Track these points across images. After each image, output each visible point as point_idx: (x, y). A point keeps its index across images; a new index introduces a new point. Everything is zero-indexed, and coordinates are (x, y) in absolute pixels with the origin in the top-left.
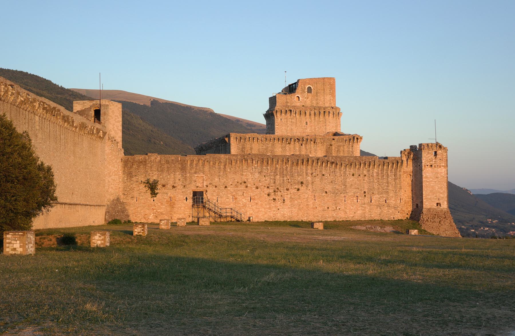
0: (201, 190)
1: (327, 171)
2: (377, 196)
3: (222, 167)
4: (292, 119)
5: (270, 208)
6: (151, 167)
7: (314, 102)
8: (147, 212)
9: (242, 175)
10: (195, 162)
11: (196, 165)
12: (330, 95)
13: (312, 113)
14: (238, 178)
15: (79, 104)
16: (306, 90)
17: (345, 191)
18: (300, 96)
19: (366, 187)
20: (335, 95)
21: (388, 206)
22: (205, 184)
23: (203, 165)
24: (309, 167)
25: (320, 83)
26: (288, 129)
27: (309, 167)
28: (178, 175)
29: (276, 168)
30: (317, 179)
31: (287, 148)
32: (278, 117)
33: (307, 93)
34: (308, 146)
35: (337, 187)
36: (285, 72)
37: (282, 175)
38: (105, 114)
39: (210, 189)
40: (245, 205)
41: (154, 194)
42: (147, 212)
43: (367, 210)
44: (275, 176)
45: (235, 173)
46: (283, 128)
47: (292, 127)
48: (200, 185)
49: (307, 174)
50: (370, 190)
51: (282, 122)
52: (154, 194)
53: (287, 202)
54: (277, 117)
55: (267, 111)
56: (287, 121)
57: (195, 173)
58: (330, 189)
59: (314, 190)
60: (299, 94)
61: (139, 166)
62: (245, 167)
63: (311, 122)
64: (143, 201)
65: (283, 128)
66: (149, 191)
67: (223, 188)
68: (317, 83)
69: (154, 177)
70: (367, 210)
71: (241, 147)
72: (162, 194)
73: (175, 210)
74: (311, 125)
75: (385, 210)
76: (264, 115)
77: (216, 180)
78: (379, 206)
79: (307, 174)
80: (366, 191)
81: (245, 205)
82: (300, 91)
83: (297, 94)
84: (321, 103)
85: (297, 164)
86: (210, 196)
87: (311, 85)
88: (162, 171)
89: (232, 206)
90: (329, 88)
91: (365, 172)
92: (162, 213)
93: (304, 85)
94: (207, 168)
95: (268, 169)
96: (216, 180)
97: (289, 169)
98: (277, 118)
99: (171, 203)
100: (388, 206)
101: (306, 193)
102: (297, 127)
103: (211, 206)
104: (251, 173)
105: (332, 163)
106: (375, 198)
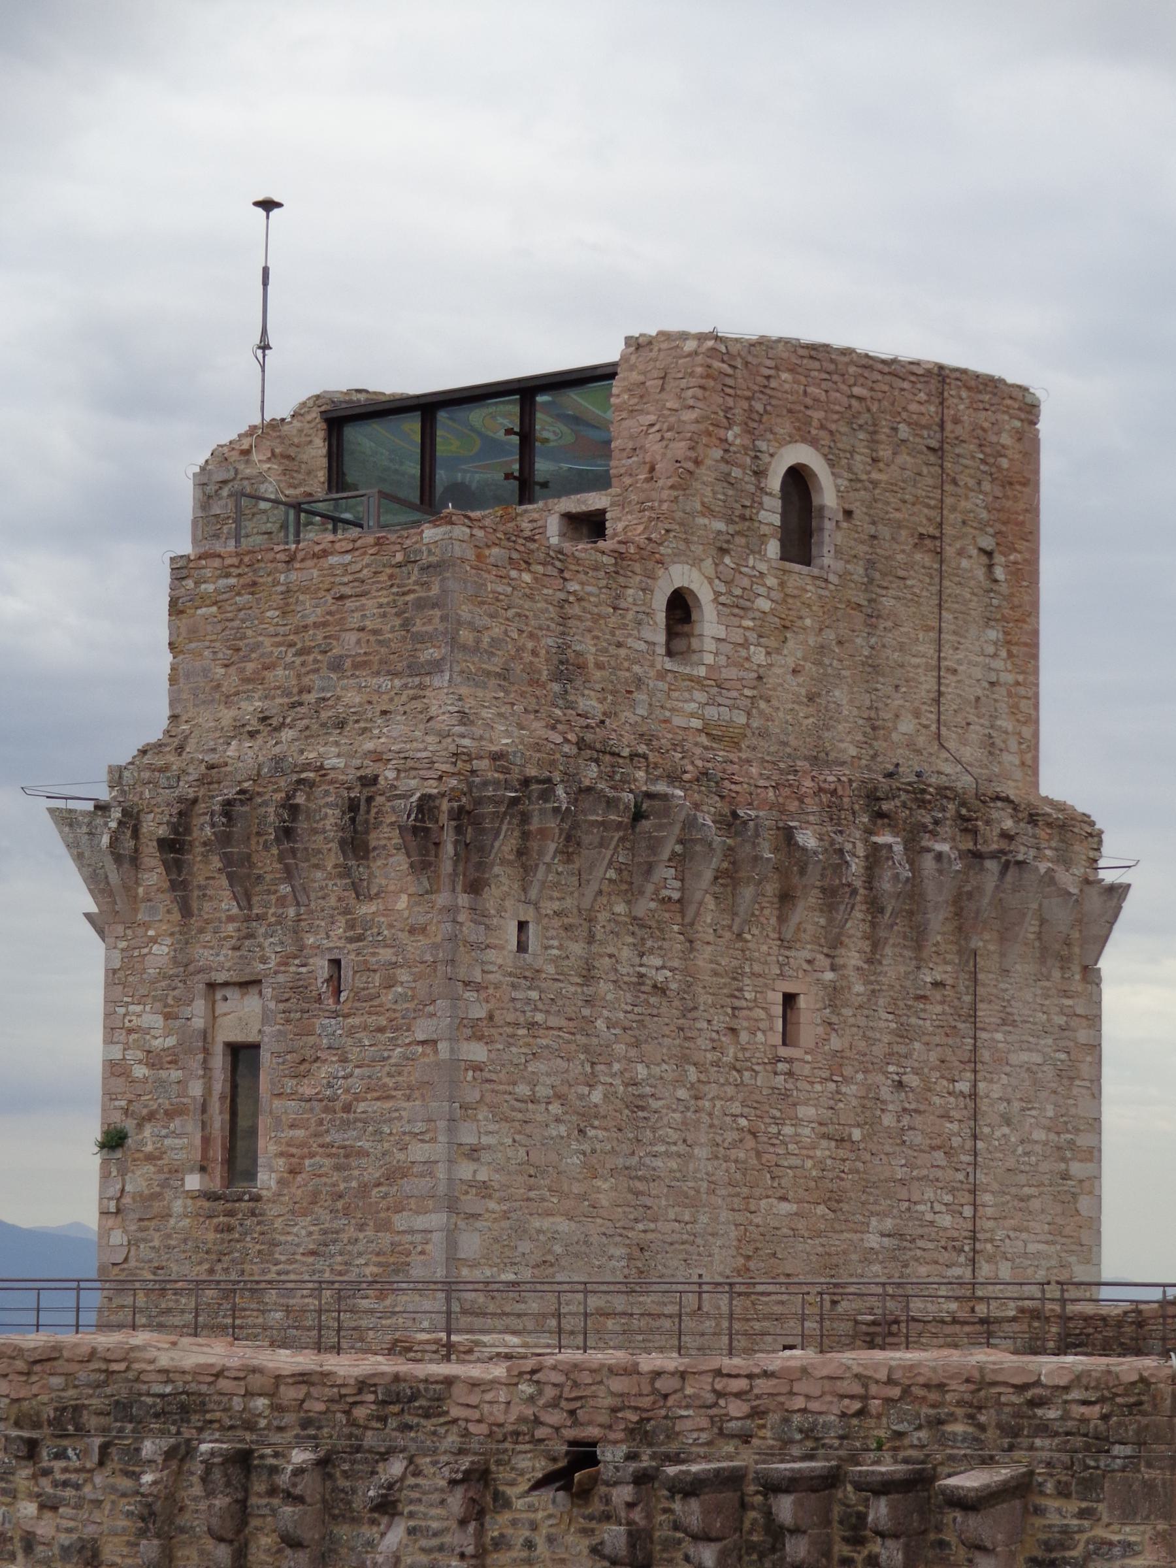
7: (839, 694)
12: (988, 621)
18: (704, 593)
20: (1036, 633)
25: (904, 431)
26: (597, 1096)
32: (491, 898)
33: (773, 548)
36: (268, 205)
47: (641, 1071)
51: (532, 977)
54: (475, 887)
55: (124, 755)
56: (588, 975)
60: (696, 562)
63: (834, 995)
68: (873, 442)
74: (836, 1043)
76: (65, 819)
82: (708, 511)
83: (677, 556)
84: (907, 726)
87: (814, 443)
90: (982, 527)
93: (754, 425)
98: (479, 915)
102: (692, 1074)
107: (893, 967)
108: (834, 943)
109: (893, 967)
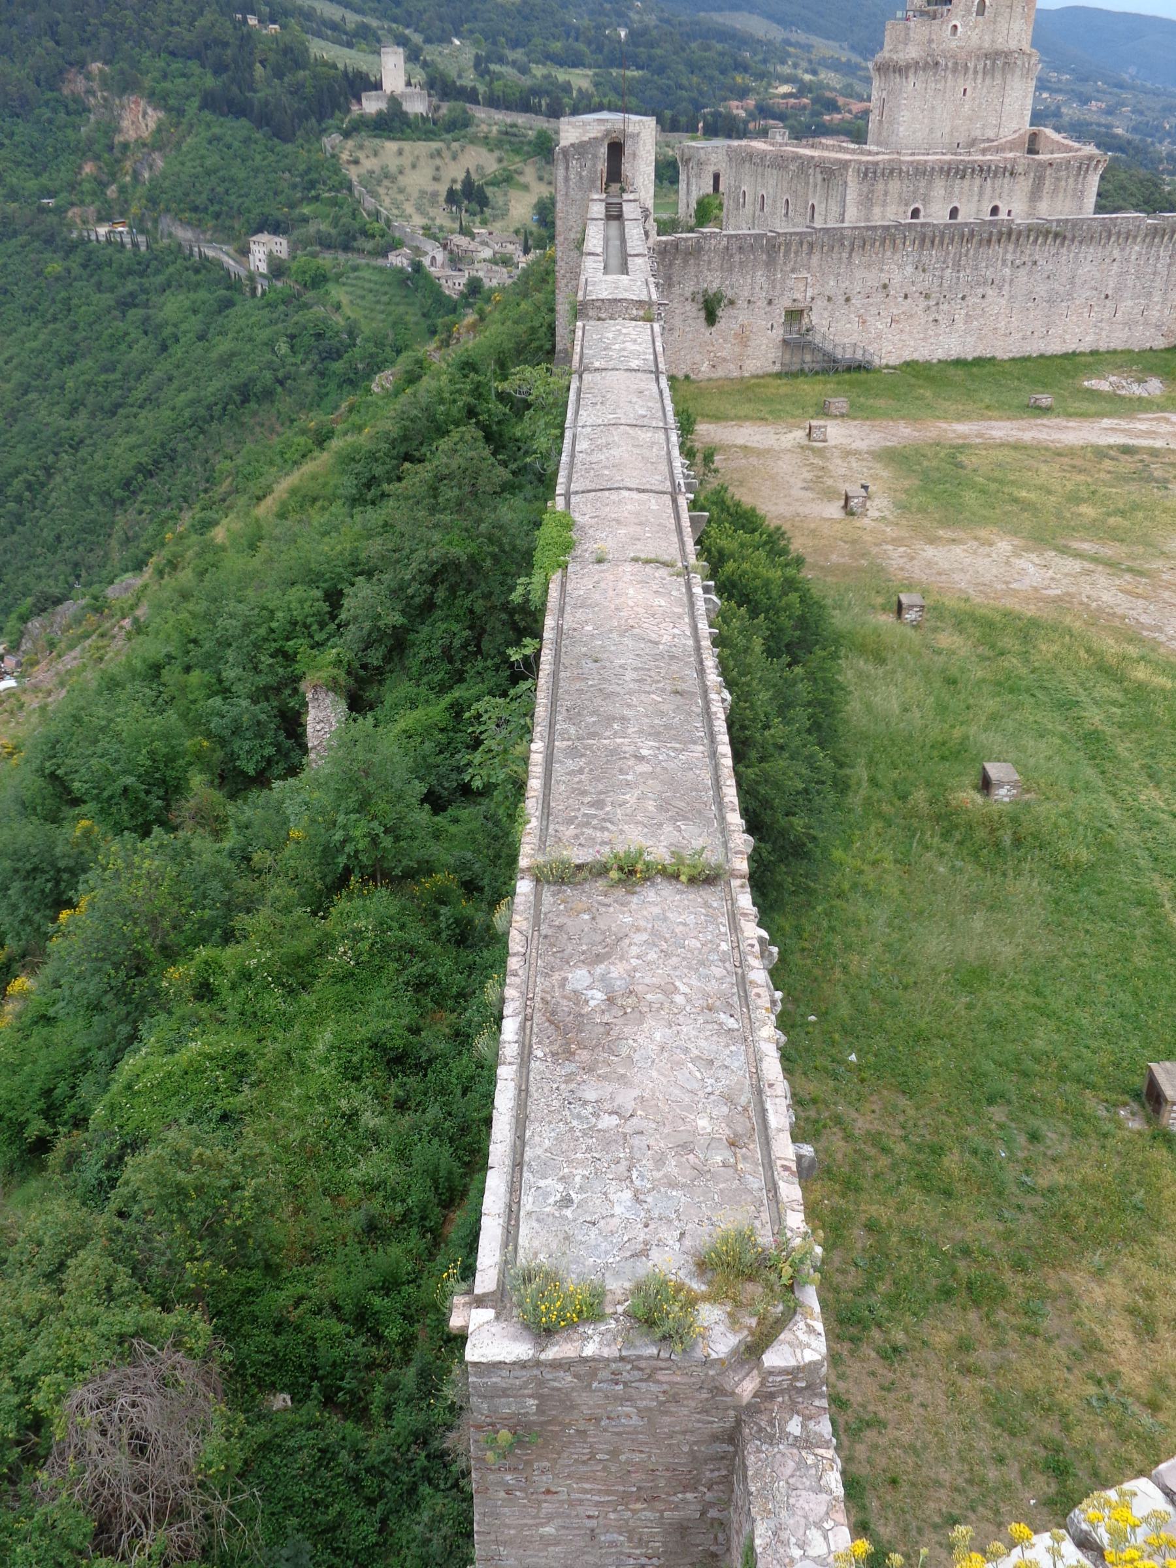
0: (801, 305)
1: (1042, 253)
2: (1130, 303)
3: (845, 255)
4: (936, 81)
5: (924, 339)
6: (710, 262)
8: (698, 358)
9: (881, 270)
10: (793, 248)
11: (796, 253)
13: (980, 67)
14: (873, 278)
15: (574, 126)
16: (975, 9)
17: (1070, 296)
19: (1112, 285)
21: (1146, 323)
22: (809, 294)
23: (810, 252)
24: (1011, 247)
27: (1011, 247)
28: (760, 276)
29: (948, 253)
30: (1023, 272)
31: (957, 190)
34: (998, 182)
35: (1056, 286)
37: (958, 267)
38: (634, 155)
39: (820, 303)
40: (879, 336)
41: (711, 318)
42: (698, 358)
43: (1104, 333)
44: (943, 270)
45: (868, 267)
46: (917, 104)
48: (798, 296)
49: (1004, 261)
50: (1117, 290)
52: (711, 318)
53: (960, 325)
57: (793, 271)
58: (1043, 294)
59: (1011, 297)
61: (686, 262)
62: (889, 253)
64: (690, 336)
65: (917, 104)
66: (703, 314)
67: (842, 299)
69: (713, 282)
70: (1104, 333)
71: (865, 190)
72: (728, 320)
73: (750, 351)
75: (1138, 331)
77: (832, 283)
78: (1129, 324)
79: (1004, 261)
80: (1110, 292)
81: (879, 336)
85: (989, 241)
86: (817, 318)
88: (730, 270)
89: (855, 338)
91: (1116, 253)
92: (724, 360)
94: (815, 260)
95: (932, 256)
96: (832, 283)
97: (972, 252)
99: (743, 338)
100: (1146, 323)
101: (997, 303)
103: (818, 339)
104: (899, 267)
105: (1056, 235)
106: (1127, 305)
107: (988, 81)
108: (975, 79)
109: (988, 81)
